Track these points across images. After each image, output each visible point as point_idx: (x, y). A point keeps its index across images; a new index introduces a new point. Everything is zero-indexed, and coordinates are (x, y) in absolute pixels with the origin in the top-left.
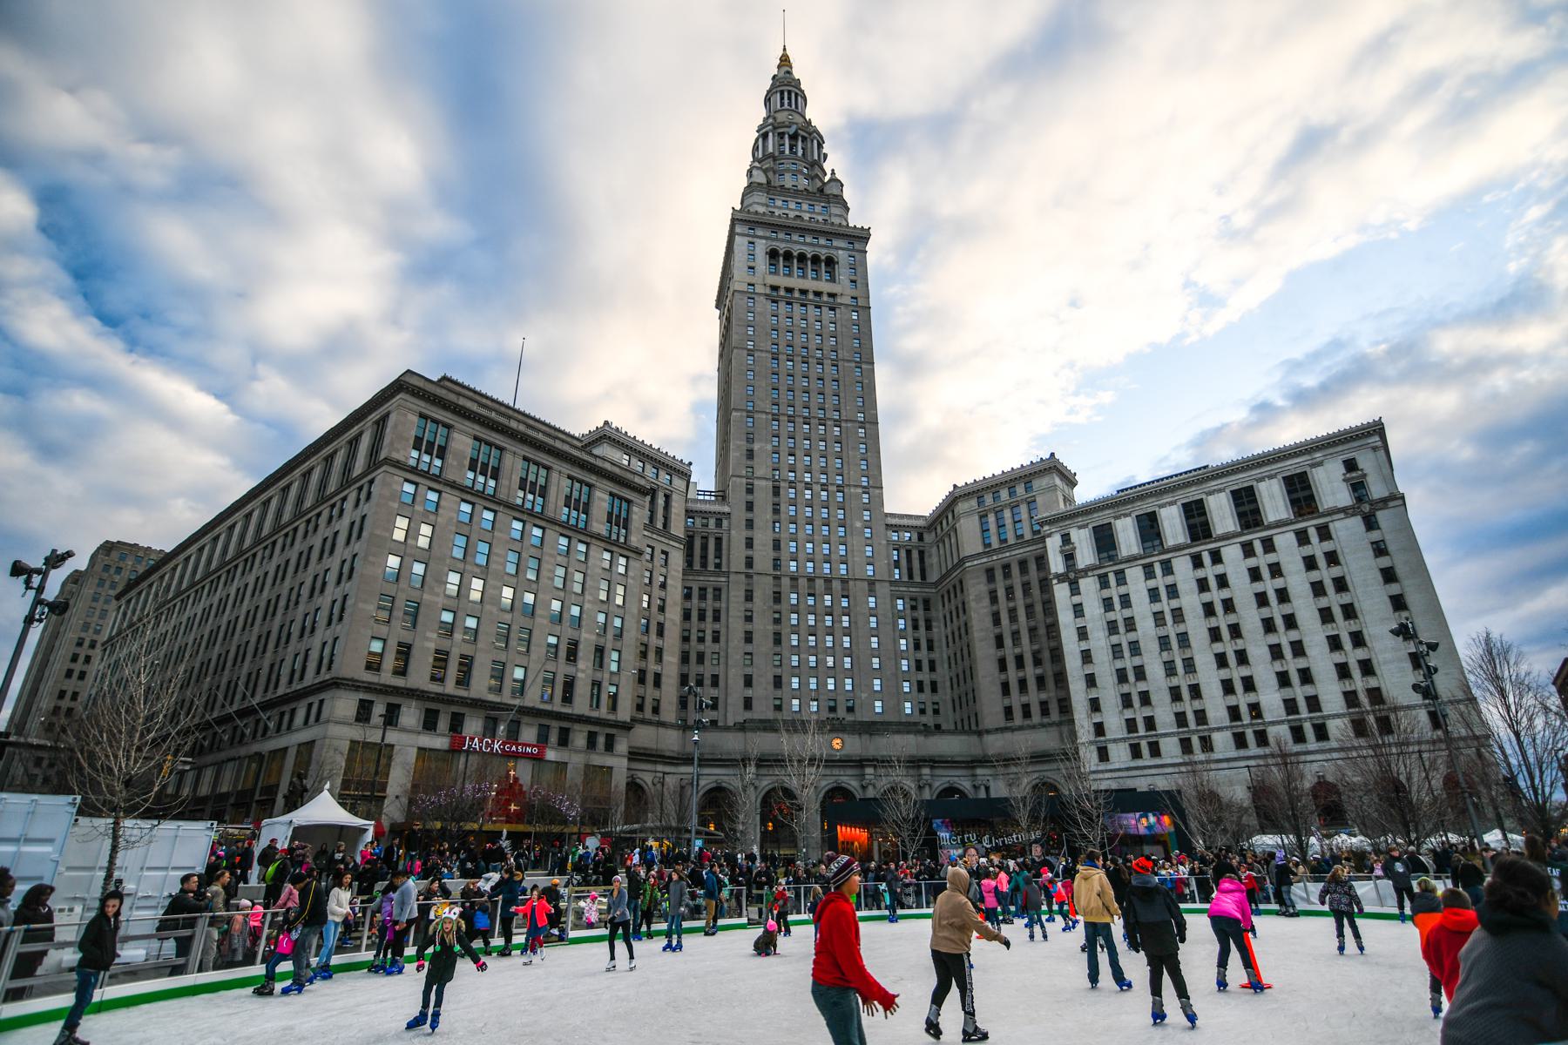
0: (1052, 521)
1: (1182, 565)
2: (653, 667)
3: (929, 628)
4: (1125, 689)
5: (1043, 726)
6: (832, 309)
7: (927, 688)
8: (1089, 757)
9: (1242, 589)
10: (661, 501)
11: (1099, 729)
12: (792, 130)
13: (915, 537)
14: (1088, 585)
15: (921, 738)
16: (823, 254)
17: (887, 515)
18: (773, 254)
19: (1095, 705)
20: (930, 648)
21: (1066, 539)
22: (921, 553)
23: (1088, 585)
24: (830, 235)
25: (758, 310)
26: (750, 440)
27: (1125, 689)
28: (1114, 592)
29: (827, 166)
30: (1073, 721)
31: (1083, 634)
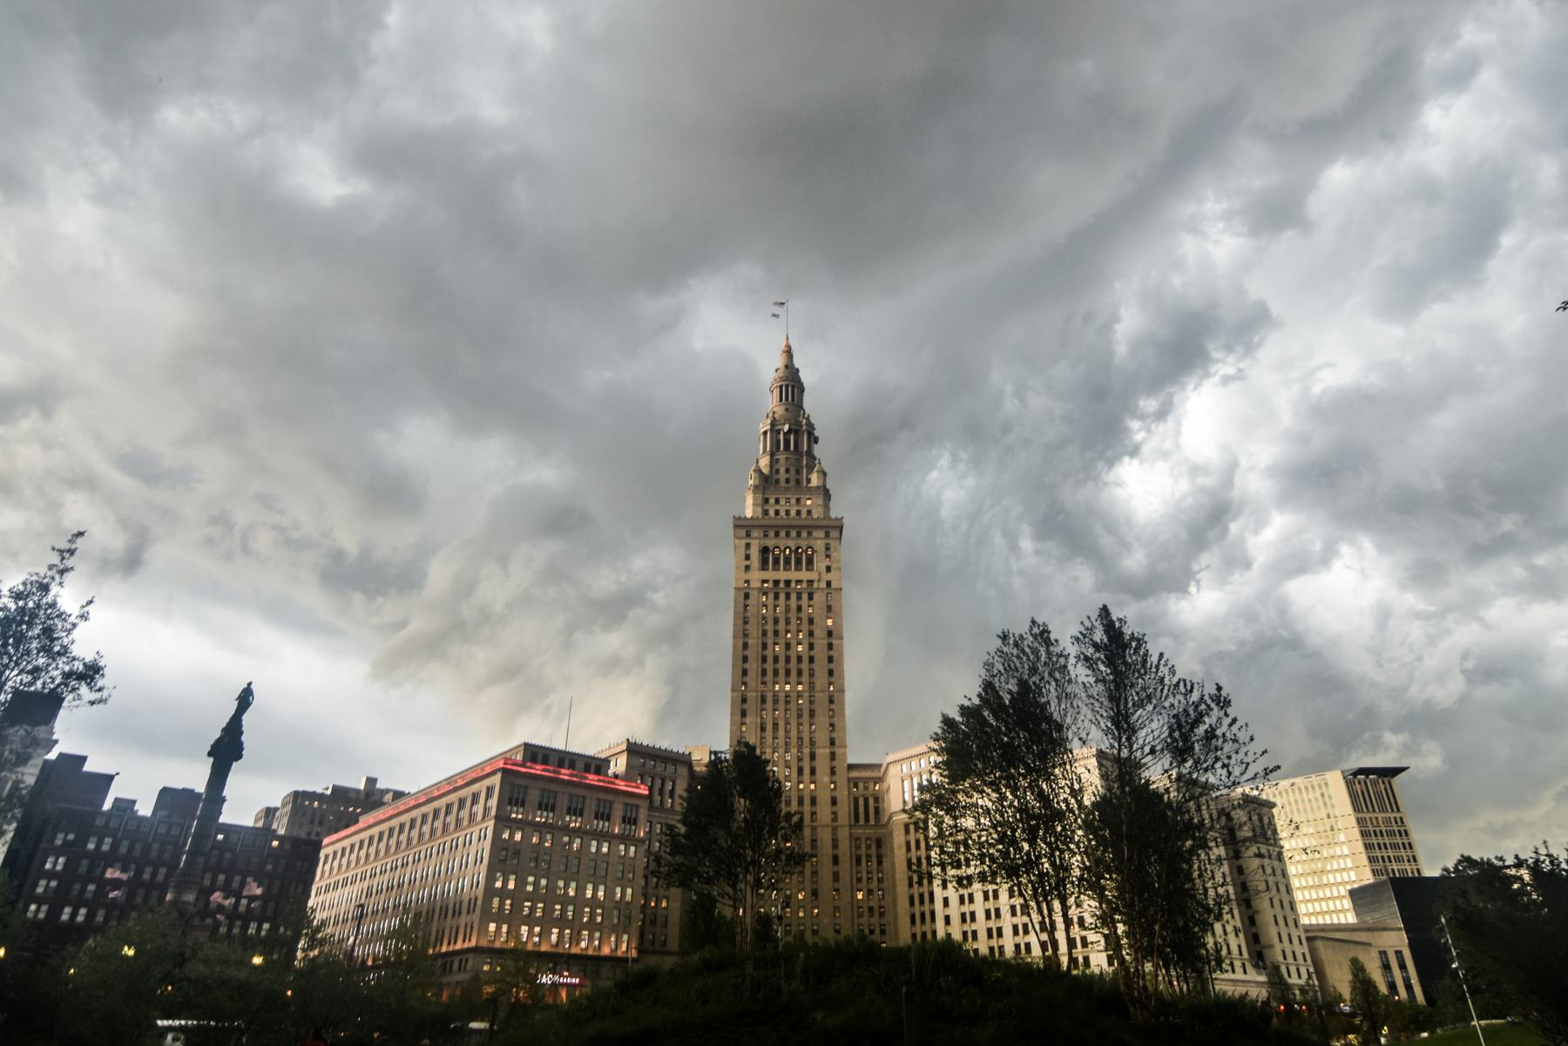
6: (811, 597)
7: (877, 914)
16: (804, 544)
17: (851, 767)
25: (752, 601)
26: (744, 714)
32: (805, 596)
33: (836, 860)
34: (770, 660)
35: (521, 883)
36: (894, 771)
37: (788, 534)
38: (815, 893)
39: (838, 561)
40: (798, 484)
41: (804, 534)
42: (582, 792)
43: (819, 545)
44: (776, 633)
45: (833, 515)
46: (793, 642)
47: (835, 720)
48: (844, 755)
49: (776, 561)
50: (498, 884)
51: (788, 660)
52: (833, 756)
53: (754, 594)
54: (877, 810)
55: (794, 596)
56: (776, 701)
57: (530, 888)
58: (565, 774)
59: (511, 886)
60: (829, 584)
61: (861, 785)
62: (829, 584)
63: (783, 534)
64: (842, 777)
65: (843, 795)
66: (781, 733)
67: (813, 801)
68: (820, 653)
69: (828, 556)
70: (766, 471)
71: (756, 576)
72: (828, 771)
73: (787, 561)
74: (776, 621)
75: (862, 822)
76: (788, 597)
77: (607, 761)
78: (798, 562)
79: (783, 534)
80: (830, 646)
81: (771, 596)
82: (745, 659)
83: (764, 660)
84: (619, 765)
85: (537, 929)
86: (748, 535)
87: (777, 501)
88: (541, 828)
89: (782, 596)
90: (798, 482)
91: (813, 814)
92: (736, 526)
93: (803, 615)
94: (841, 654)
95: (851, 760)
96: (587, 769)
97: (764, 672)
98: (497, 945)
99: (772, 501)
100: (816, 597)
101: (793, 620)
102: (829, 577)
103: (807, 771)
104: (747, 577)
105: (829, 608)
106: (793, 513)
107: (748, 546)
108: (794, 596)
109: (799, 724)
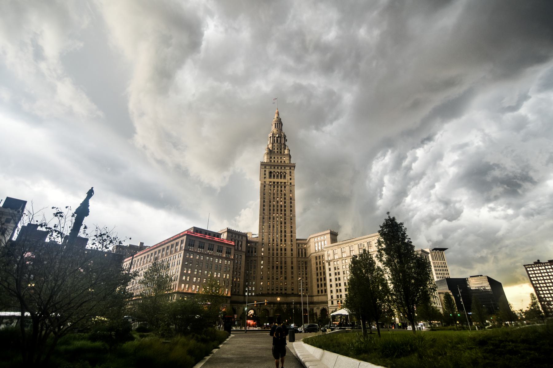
3: (306, 269)
4: (337, 288)
5: (324, 295)
8: (330, 303)
11: (332, 297)
12: (277, 136)
16: (283, 171)
17: (297, 240)
18: (270, 173)
19: (331, 291)
20: (306, 274)
23: (331, 263)
24: (285, 166)
25: (266, 188)
26: (263, 223)
27: (337, 288)
29: (287, 143)
30: (327, 295)
31: (330, 275)
32: (283, 187)
33: (292, 268)
34: (272, 206)
35: (193, 271)
36: (312, 240)
37: (278, 168)
38: (286, 278)
39: (294, 177)
40: (281, 153)
41: (283, 168)
42: (213, 243)
43: (288, 172)
44: (274, 198)
45: (292, 162)
46: (279, 201)
47: (292, 225)
48: (295, 236)
49: (274, 176)
50: (185, 272)
51: (277, 206)
52: (291, 236)
53: (267, 186)
54: (305, 253)
55: (279, 187)
56: (274, 219)
57: (196, 273)
58: (207, 237)
59: (189, 272)
60: (291, 183)
62: (291, 183)
63: (276, 168)
64: (294, 243)
65: (294, 247)
66: (275, 229)
67: (285, 250)
68: (288, 204)
69: (290, 175)
70: (271, 149)
71: (268, 180)
73: (278, 176)
74: (274, 194)
75: (300, 256)
76: (278, 187)
77: (221, 234)
78: (281, 177)
79: (276, 168)
80: (291, 203)
81: (272, 186)
82: (264, 206)
83: (270, 206)
84: (224, 236)
85: (198, 287)
86: (265, 168)
87: (274, 158)
88: (200, 254)
89: (276, 187)
90: (281, 152)
91: (285, 254)
92: (261, 165)
93: (282, 193)
94: (294, 205)
96: (214, 236)
97: (270, 210)
98: (185, 291)
99: (273, 158)
100: (287, 187)
101: (279, 194)
102: (291, 181)
103: (283, 240)
104: (265, 180)
105: (291, 191)
106: (279, 162)
107: (265, 171)
108: (279, 187)
109: (281, 226)
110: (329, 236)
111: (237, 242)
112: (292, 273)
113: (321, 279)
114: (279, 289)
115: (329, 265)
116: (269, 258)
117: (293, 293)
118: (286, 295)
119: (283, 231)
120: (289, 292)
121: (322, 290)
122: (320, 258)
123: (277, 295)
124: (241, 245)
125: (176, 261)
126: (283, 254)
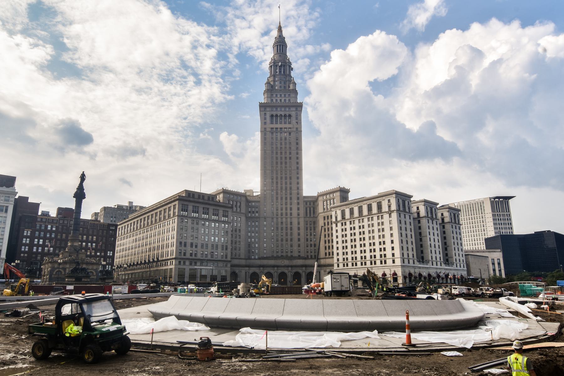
0: (334, 208)
1: (357, 222)
2: (238, 246)
4: (344, 251)
9: (366, 229)
10: (239, 204)
11: (338, 260)
13: (312, 204)
14: (339, 224)
15: (304, 260)
17: (305, 197)
19: (338, 254)
21: (336, 213)
22: (314, 208)
23: (339, 224)
27: (344, 251)
28: (344, 227)
33: (299, 229)
61: (308, 203)
65: (302, 206)
72: (296, 198)
95: (304, 195)
110: (338, 194)
111: (235, 203)
112: (299, 234)
113: (329, 241)
114: (284, 251)
115: (337, 226)
116: (273, 218)
117: (299, 256)
118: (292, 258)
119: (288, 189)
120: (296, 254)
121: (329, 253)
122: (328, 218)
123: (282, 257)
124: (240, 206)
125: (171, 226)
126: (289, 214)
